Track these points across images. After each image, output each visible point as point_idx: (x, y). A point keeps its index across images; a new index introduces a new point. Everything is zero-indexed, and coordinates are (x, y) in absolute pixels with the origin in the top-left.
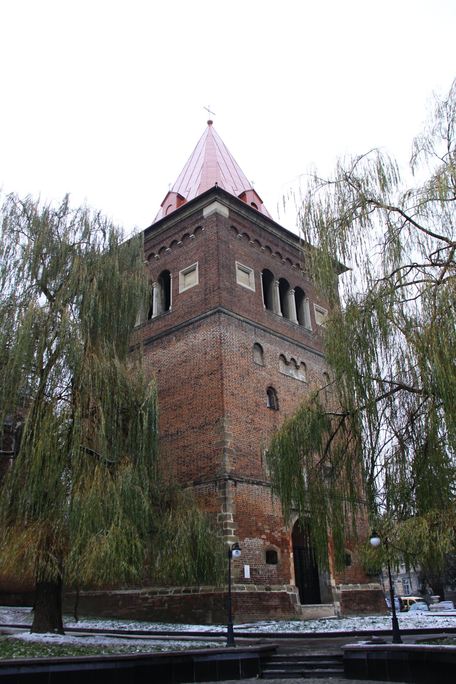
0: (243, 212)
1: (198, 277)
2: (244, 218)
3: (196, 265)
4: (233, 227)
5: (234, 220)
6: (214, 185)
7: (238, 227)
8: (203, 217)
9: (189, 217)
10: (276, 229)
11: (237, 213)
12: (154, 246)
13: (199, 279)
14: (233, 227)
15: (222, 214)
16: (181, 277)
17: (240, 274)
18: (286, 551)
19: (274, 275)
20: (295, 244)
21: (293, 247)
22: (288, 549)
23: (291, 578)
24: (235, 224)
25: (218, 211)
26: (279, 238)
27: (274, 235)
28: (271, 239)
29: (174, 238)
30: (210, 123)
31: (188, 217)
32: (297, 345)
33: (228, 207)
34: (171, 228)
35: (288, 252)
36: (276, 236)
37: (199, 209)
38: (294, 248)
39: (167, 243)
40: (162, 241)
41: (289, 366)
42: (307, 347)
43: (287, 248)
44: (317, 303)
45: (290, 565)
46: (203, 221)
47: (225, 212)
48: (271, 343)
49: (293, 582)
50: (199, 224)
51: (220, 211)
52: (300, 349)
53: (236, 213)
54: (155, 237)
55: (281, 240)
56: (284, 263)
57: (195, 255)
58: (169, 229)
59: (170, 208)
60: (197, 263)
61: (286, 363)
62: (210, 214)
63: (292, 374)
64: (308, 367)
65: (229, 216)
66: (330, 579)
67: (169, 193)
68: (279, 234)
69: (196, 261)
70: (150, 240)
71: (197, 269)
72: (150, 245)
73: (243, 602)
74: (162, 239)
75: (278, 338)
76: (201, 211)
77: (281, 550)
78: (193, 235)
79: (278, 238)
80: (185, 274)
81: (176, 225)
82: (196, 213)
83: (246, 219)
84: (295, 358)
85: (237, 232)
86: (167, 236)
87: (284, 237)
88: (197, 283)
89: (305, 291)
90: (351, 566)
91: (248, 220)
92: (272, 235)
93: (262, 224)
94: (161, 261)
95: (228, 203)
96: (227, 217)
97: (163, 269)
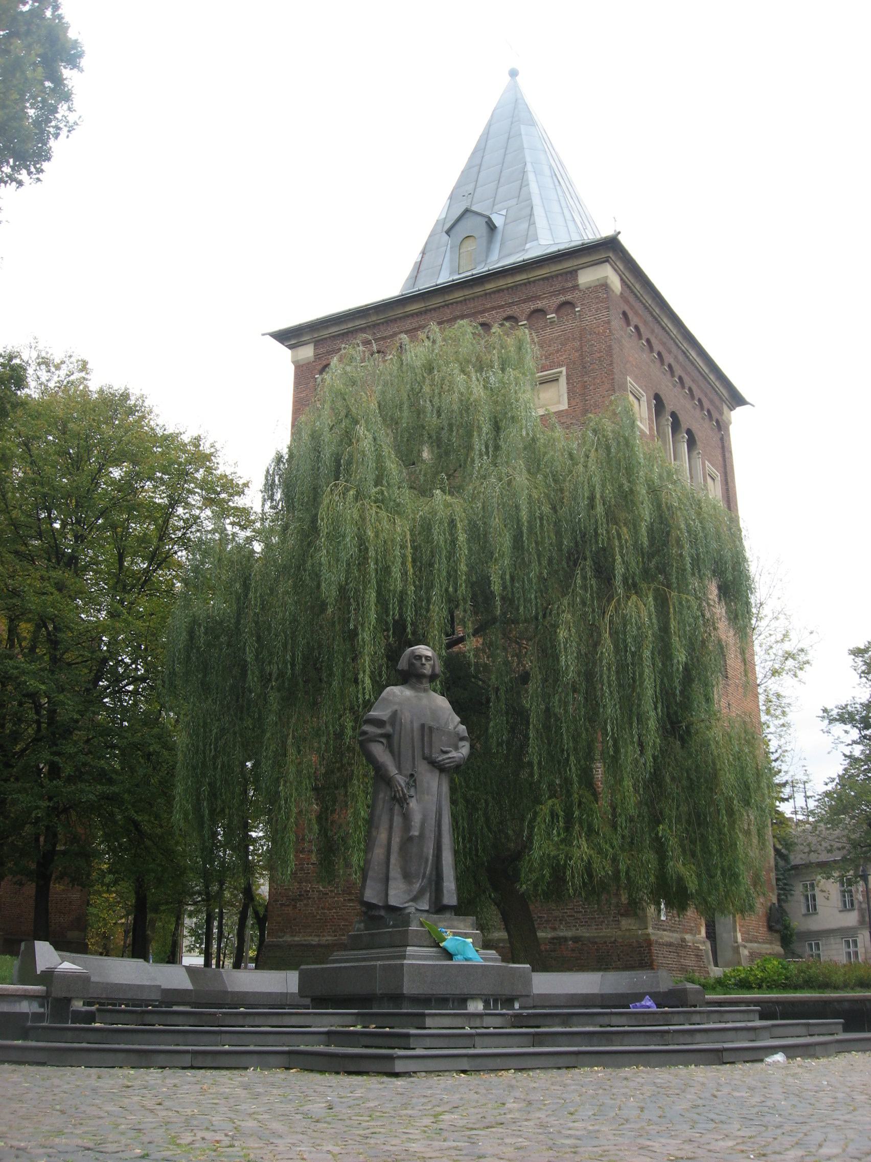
1: (566, 395)
3: (561, 372)
5: (627, 302)
7: (630, 315)
8: (578, 285)
9: (547, 279)
13: (569, 400)
20: (690, 351)
25: (609, 282)
26: (672, 339)
28: (665, 340)
29: (509, 312)
30: (513, 73)
31: (543, 279)
33: (620, 276)
34: (503, 290)
36: (668, 333)
37: (571, 269)
38: (688, 357)
40: (483, 312)
44: (709, 462)
46: (577, 294)
47: (616, 283)
50: (568, 297)
54: (465, 300)
57: (557, 351)
58: (499, 291)
59: (470, 241)
60: (564, 369)
62: (593, 285)
65: (621, 293)
66: (735, 931)
67: (467, 211)
68: (674, 331)
69: (562, 366)
70: (452, 304)
71: (563, 380)
72: (451, 313)
73: (664, 957)
74: (480, 308)
76: (573, 273)
78: (554, 315)
82: (561, 275)
85: (628, 324)
86: (495, 304)
87: (679, 337)
88: (564, 406)
92: (666, 331)
95: (621, 268)
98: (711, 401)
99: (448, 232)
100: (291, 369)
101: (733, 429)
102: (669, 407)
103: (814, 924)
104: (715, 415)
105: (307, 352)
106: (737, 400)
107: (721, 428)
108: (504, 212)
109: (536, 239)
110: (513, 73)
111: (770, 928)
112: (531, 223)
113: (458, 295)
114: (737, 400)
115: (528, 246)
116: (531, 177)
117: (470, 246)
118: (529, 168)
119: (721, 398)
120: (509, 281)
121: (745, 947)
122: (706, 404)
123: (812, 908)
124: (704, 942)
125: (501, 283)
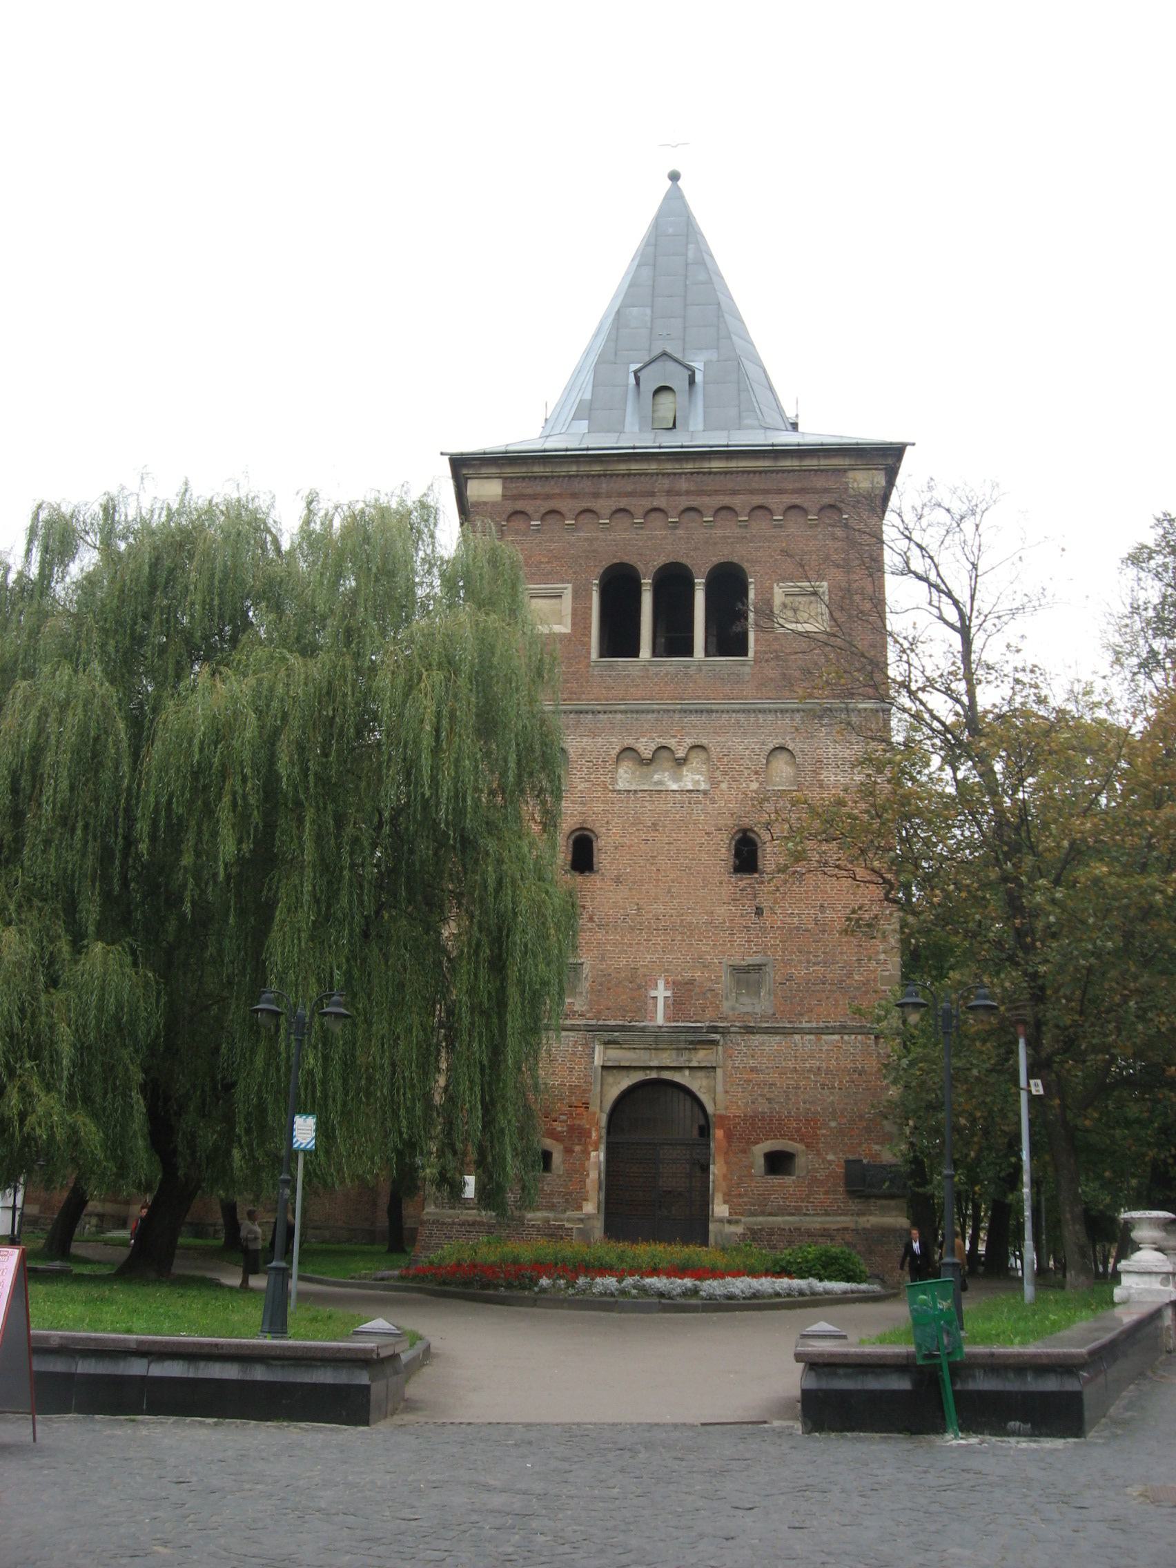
2: (547, 477)
5: (515, 498)
6: (446, 458)
10: (636, 461)
11: (527, 477)
15: (484, 500)
18: (578, 1148)
19: (640, 567)
21: (704, 473)
22: (585, 1145)
23: (586, 1200)
24: (519, 505)
26: (657, 474)
27: (641, 475)
30: (674, 177)
32: (680, 711)
35: (688, 493)
36: (647, 474)
38: (710, 473)
41: (652, 768)
42: (714, 707)
43: (683, 485)
45: (588, 1175)
49: (590, 1208)
51: (479, 496)
52: (693, 718)
53: (524, 478)
55: (663, 474)
56: (675, 526)
63: (660, 782)
64: (714, 751)
65: (503, 496)
68: (653, 467)
75: (619, 716)
77: (565, 1148)
79: (652, 475)
83: (553, 477)
84: (672, 743)
89: (745, 565)
90: (794, 1178)
91: (559, 477)
92: (635, 475)
93: (597, 468)
96: (499, 499)
110: (674, 177)
119: (839, 470)
121: (737, 1222)
124: (581, 1220)
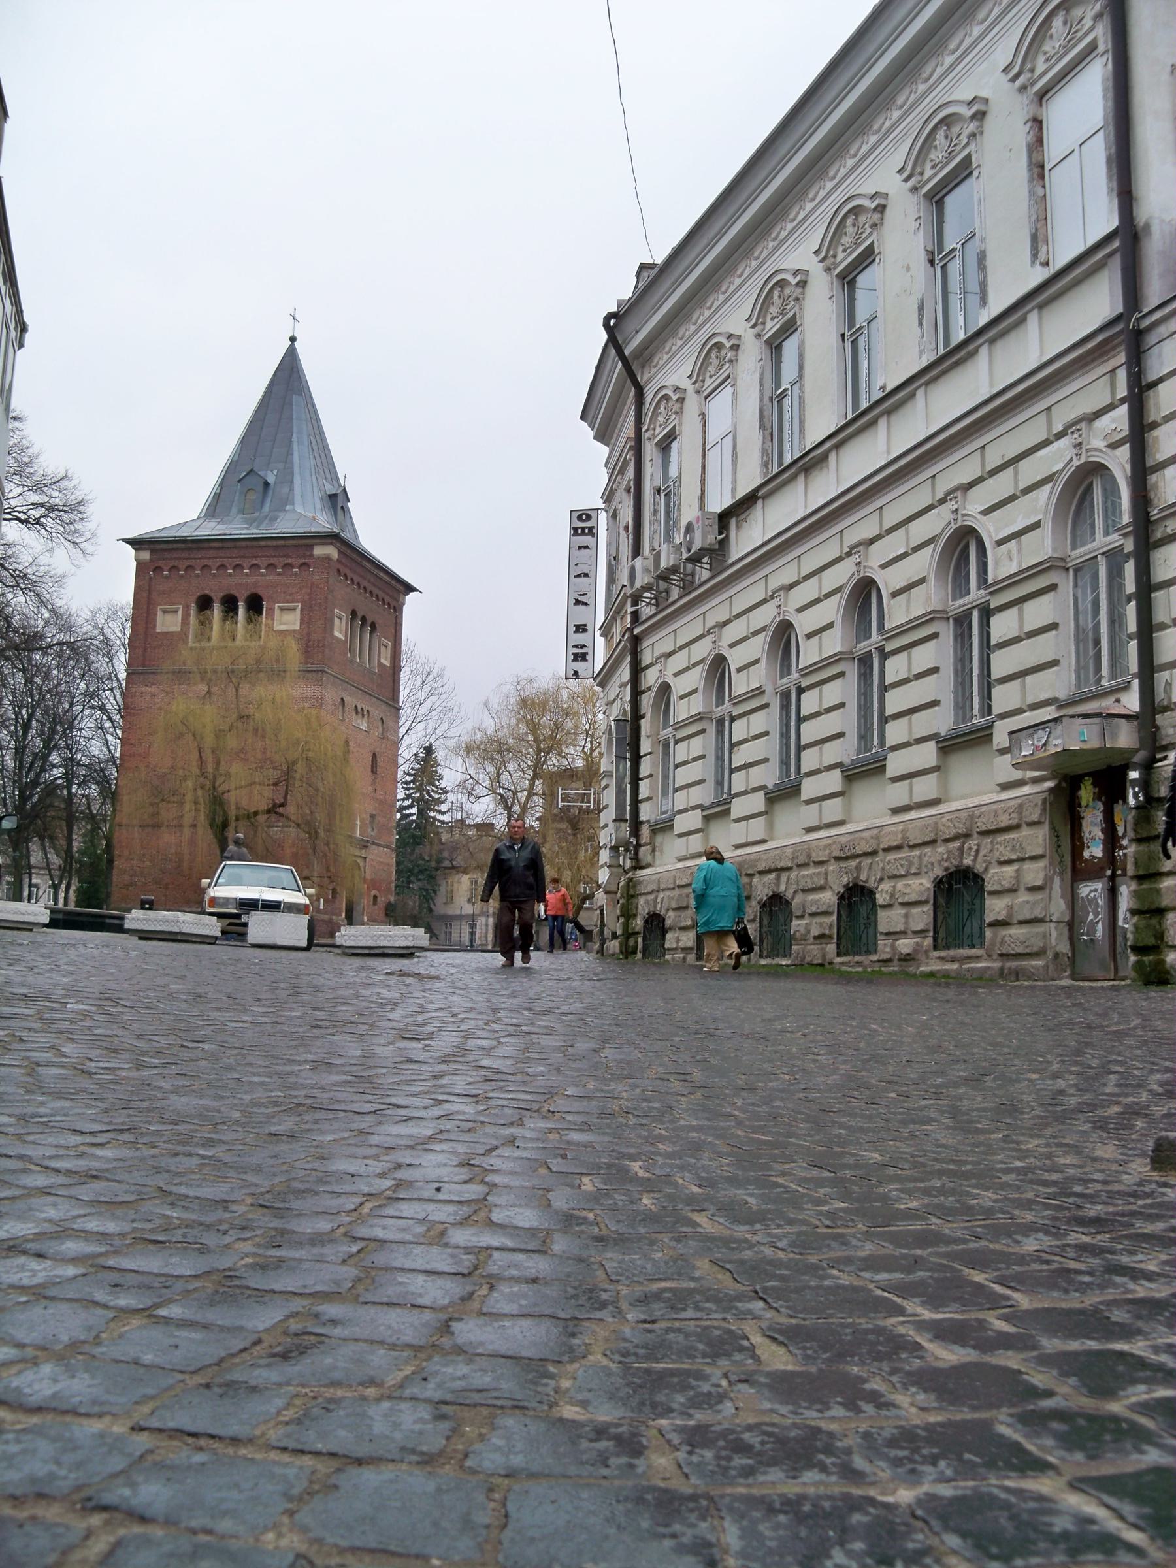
0: (348, 552)
4: (339, 570)
12: (244, 557)
14: (339, 570)
16: (277, 611)
17: (337, 621)
29: (272, 561)
30: (293, 339)
39: (263, 562)
46: (312, 560)
48: (350, 695)
49: (344, 915)
61: (357, 713)
67: (252, 471)
71: (298, 611)
76: (311, 547)
80: (282, 609)
81: (277, 547)
88: (297, 627)
94: (252, 580)
97: (253, 590)
98: (392, 597)
99: (239, 481)
100: (134, 563)
101: (407, 611)
102: (360, 615)
103: (453, 911)
104: (393, 603)
105: (146, 555)
106: (410, 589)
107: (397, 610)
108: (275, 472)
109: (293, 504)
110: (293, 339)
111: (387, 915)
112: (292, 490)
113: (244, 544)
114: (410, 589)
115: (288, 507)
116: (295, 447)
117: (252, 496)
118: (295, 438)
120: (275, 543)
122: (387, 599)
123: (451, 899)
125: (269, 543)
